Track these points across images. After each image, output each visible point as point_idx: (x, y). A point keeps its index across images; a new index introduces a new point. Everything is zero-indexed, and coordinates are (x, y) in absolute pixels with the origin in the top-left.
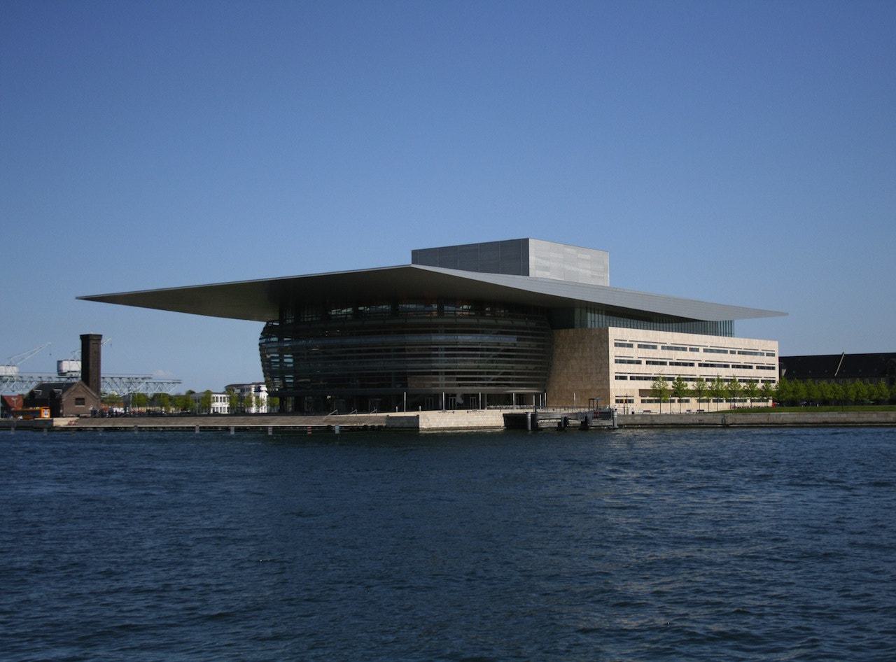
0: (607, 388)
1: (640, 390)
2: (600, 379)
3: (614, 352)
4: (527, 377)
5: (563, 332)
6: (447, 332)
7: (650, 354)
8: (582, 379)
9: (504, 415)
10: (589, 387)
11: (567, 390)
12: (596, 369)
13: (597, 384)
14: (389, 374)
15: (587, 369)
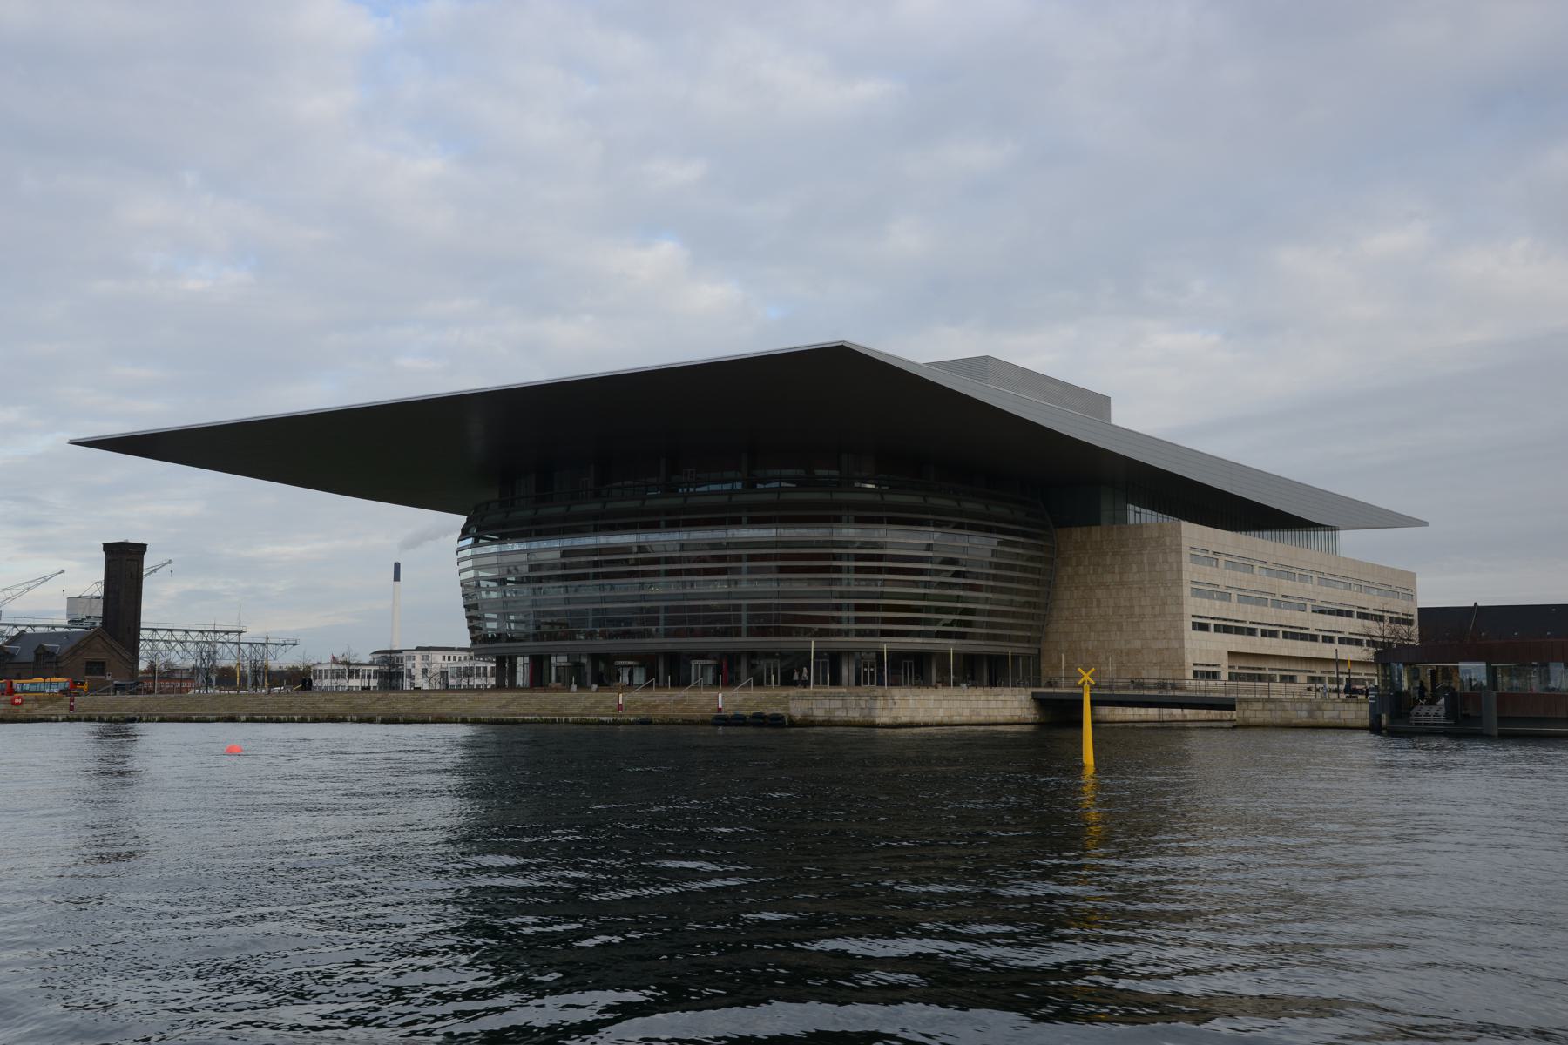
0: (1175, 645)
1: (1229, 652)
2: (1163, 628)
3: (1191, 572)
4: (1012, 621)
5: (1078, 533)
6: (860, 520)
7: (1242, 579)
8: (1120, 630)
9: (1033, 694)
10: (1137, 644)
11: (1087, 649)
12: (1153, 608)
13: (1155, 639)
14: (738, 608)
15: (1132, 607)
